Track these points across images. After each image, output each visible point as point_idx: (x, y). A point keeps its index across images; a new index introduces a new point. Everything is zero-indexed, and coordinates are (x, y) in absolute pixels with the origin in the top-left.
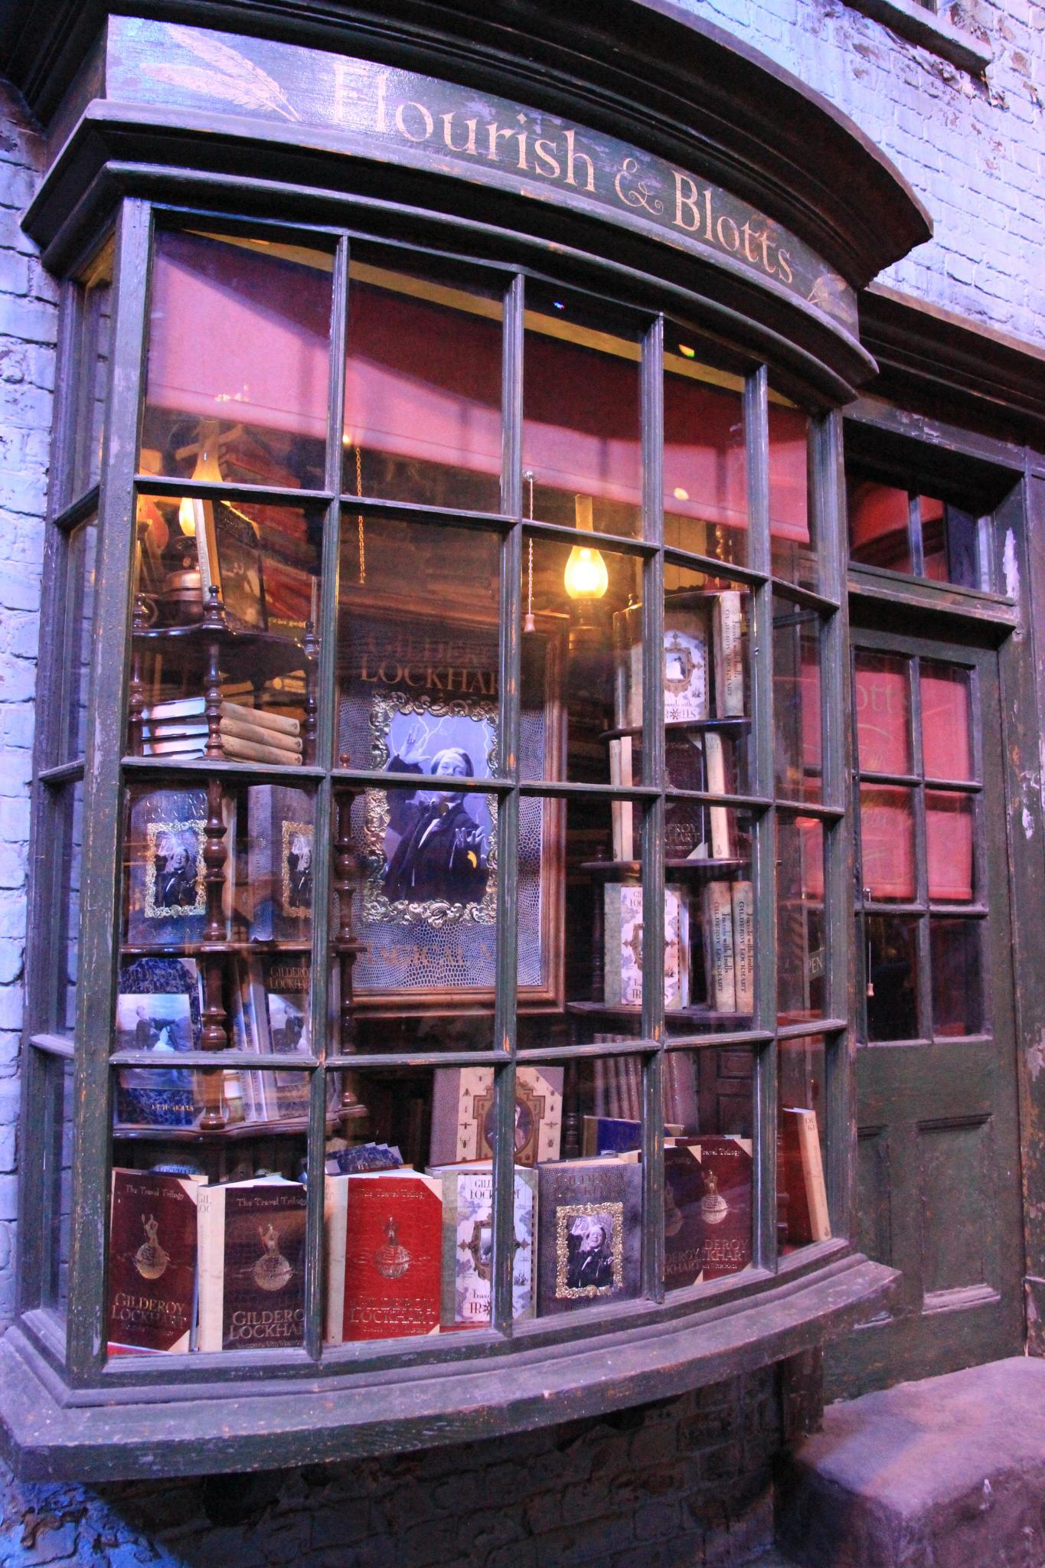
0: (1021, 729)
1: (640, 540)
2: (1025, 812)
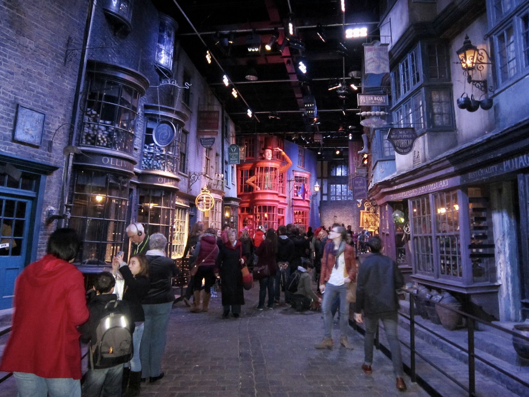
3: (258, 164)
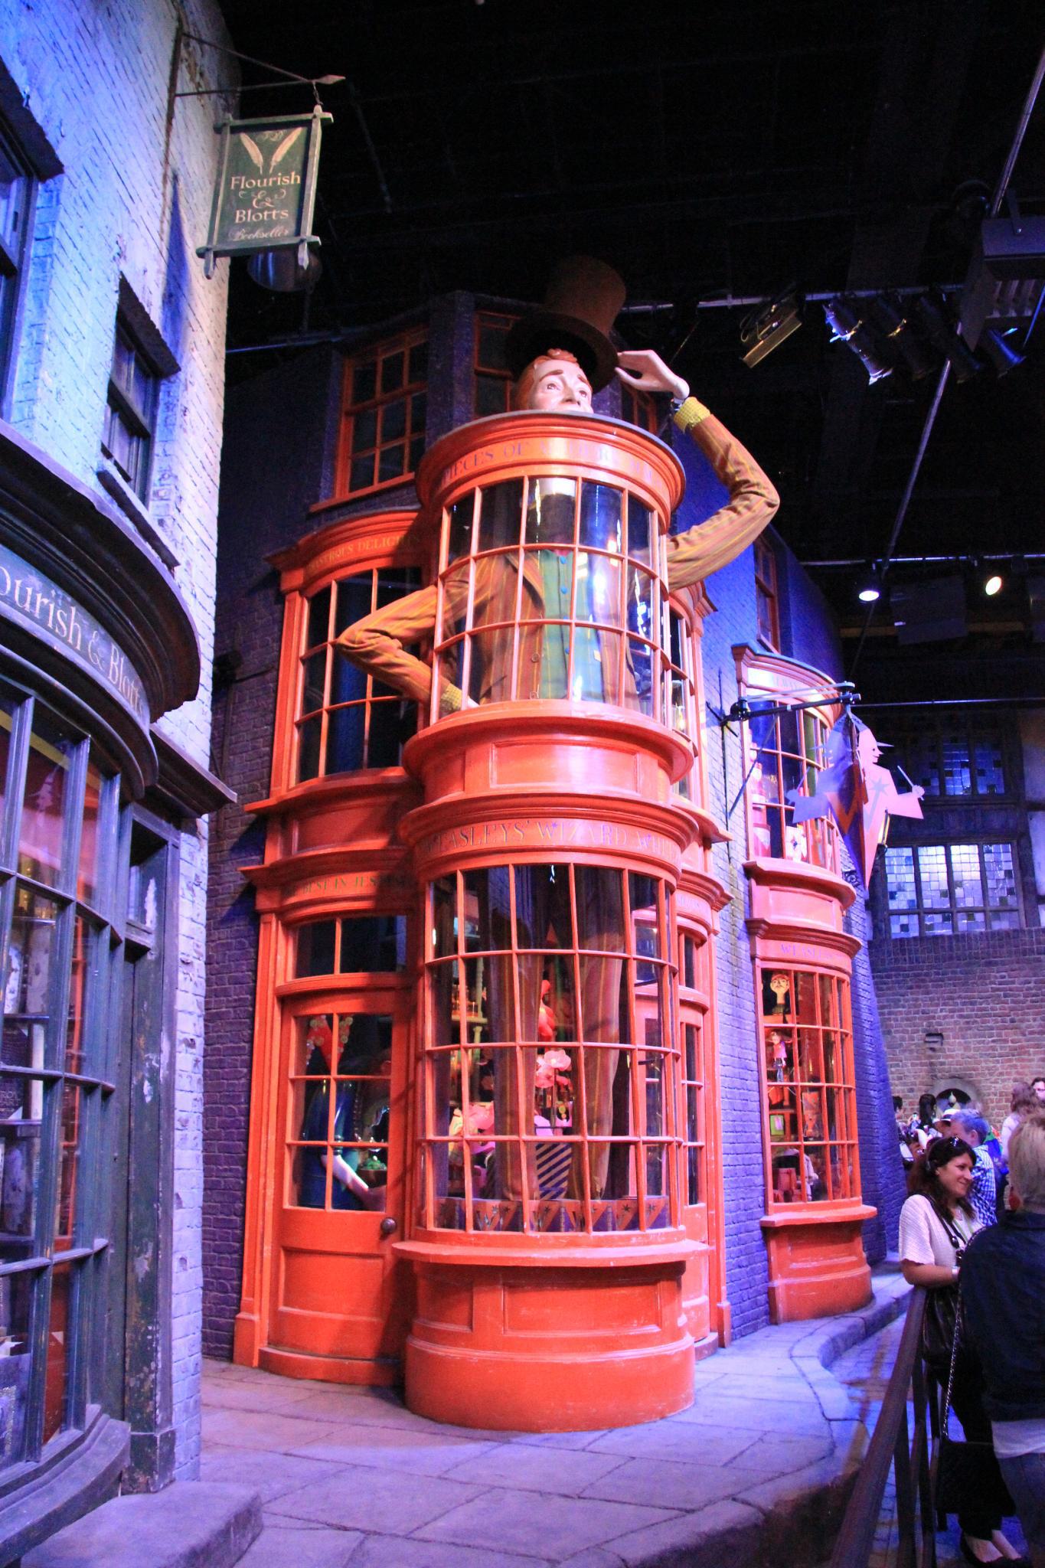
0: (148, 1023)
1: (59, 891)
2: (146, 1083)
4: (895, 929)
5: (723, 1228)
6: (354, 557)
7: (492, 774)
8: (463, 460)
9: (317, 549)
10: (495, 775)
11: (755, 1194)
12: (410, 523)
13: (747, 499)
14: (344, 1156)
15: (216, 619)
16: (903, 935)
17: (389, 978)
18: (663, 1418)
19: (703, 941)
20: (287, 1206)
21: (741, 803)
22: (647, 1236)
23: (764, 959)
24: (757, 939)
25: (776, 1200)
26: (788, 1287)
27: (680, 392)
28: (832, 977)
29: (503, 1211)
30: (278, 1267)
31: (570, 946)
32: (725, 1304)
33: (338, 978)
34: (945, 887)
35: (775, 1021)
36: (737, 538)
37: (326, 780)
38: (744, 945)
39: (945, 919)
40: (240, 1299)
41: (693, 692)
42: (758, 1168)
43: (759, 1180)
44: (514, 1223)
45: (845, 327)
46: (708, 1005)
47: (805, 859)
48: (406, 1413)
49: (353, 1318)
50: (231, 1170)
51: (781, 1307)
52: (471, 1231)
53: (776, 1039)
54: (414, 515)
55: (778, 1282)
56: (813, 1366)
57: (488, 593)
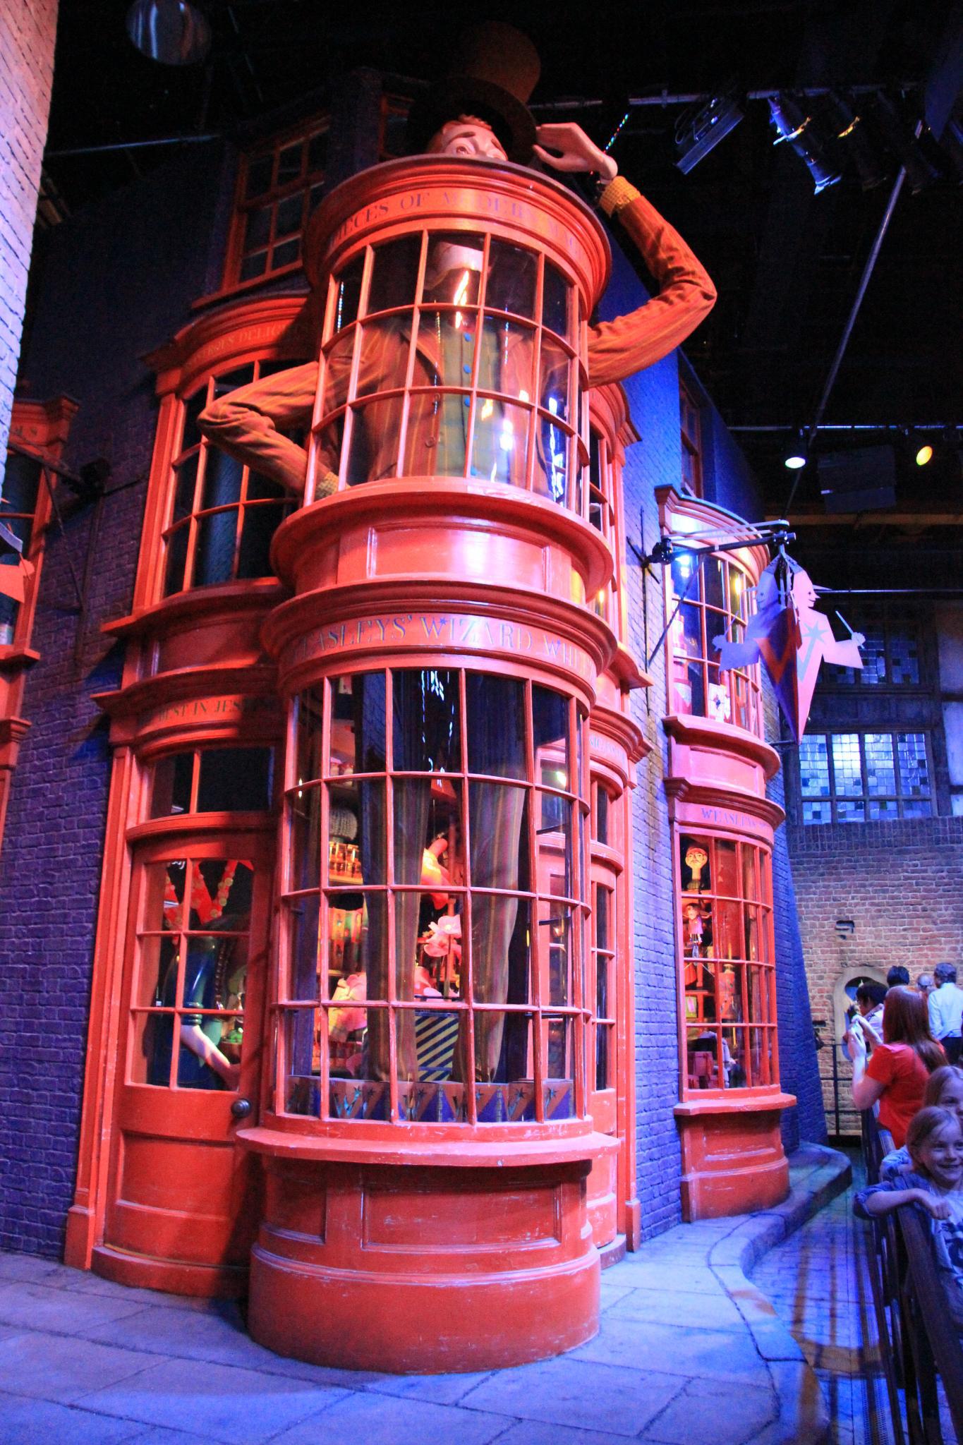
3: (361, 220)
4: (808, 816)
5: (634, 1116)
6: (234, 349)
7: (369, 562)
8: (354, 218)
9: (197, 341)
10: (374, 564)
11: (668, 1080)
12: (297, 310)
13: (681, 288)
14: (202, 1026)
15: (23, 342)
16: (816, 822)
17: (253, 819)
18: (560, 1353)
19: (617, 795)
20: (129, 1082)
21: (660, 653)
22: (546, 1128)
23: (682, 824)
24: (676, 801)
25: (691, 1086)
26: (703, 1182)
27: (606, 169)
28: (754, 847)
29: (367, 1094)
30: (117, 1151)
31: (460, 770)
32: (634, 1202)
33: (196, 818)
34: (858, 774)
35: (693, 893)
36: (666, 332)
37: (191, 591)
38: (662, 807)
39: (857, 807)
40: (74, 1189)
41: (613, 522)
42: (673, 1051)
43: (674, 1064)
44: (380, 1111)
45: (791, 126)
46: (623, 865)
47: (729, 721)
48: (244, 1339)
49: (199, 1217)
50: (71, 1040)
51: (694, 1203)
52: (327, 1118)
53: (692, 913)
54: (302, 301)
55: (692, 1177)
56: (735, 1278)
57: (378, 373)
